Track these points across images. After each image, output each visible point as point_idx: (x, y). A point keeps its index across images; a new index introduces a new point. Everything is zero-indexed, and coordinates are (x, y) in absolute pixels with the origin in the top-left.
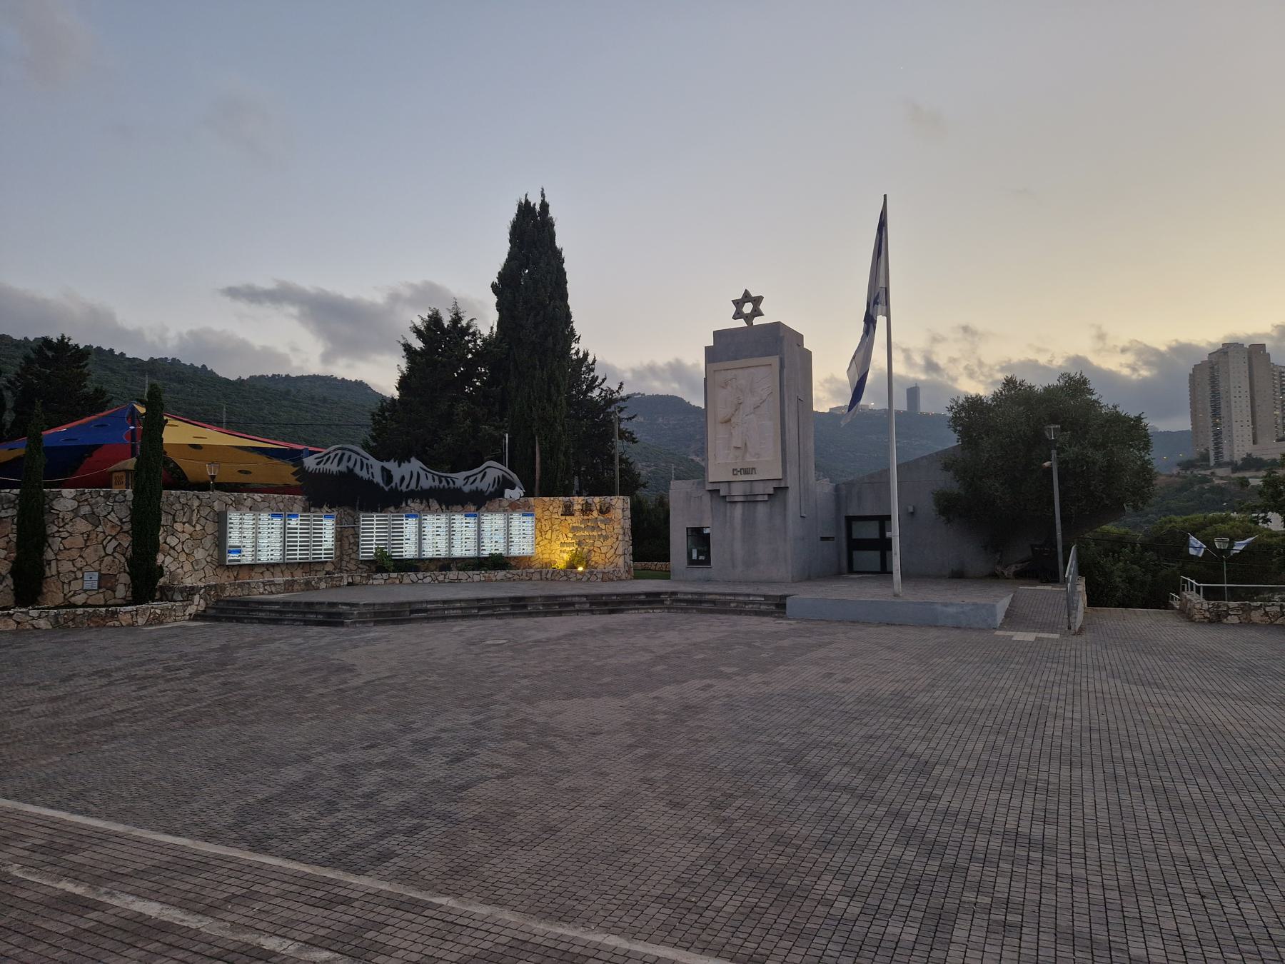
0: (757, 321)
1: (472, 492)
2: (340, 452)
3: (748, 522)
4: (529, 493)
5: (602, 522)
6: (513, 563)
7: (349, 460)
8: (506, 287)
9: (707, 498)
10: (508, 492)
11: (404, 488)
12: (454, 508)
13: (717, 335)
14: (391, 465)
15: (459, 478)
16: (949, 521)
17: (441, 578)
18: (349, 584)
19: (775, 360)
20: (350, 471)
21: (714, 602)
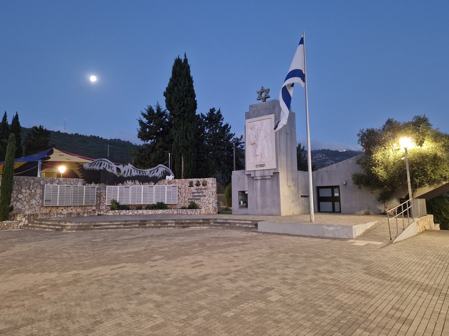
0: (267, 100)
1: (152, 177)
2: (100, 162)
3: (263, 188)
4: (175, 178)
5: (204, 189)
6: (169, 206)
7: (104, 165)
8: (169, 93)
9: (246, 178)
10: (167, 177)
11: (125, 176)
12: (145, 184)
13: (251, 107)
14: (120, 167)
15: (148, 172)
16: (360, 188)
17: (136, 213)
18: (98, 215)
19: (272, 116)
20: (104, 169)
21: (230, 223)
